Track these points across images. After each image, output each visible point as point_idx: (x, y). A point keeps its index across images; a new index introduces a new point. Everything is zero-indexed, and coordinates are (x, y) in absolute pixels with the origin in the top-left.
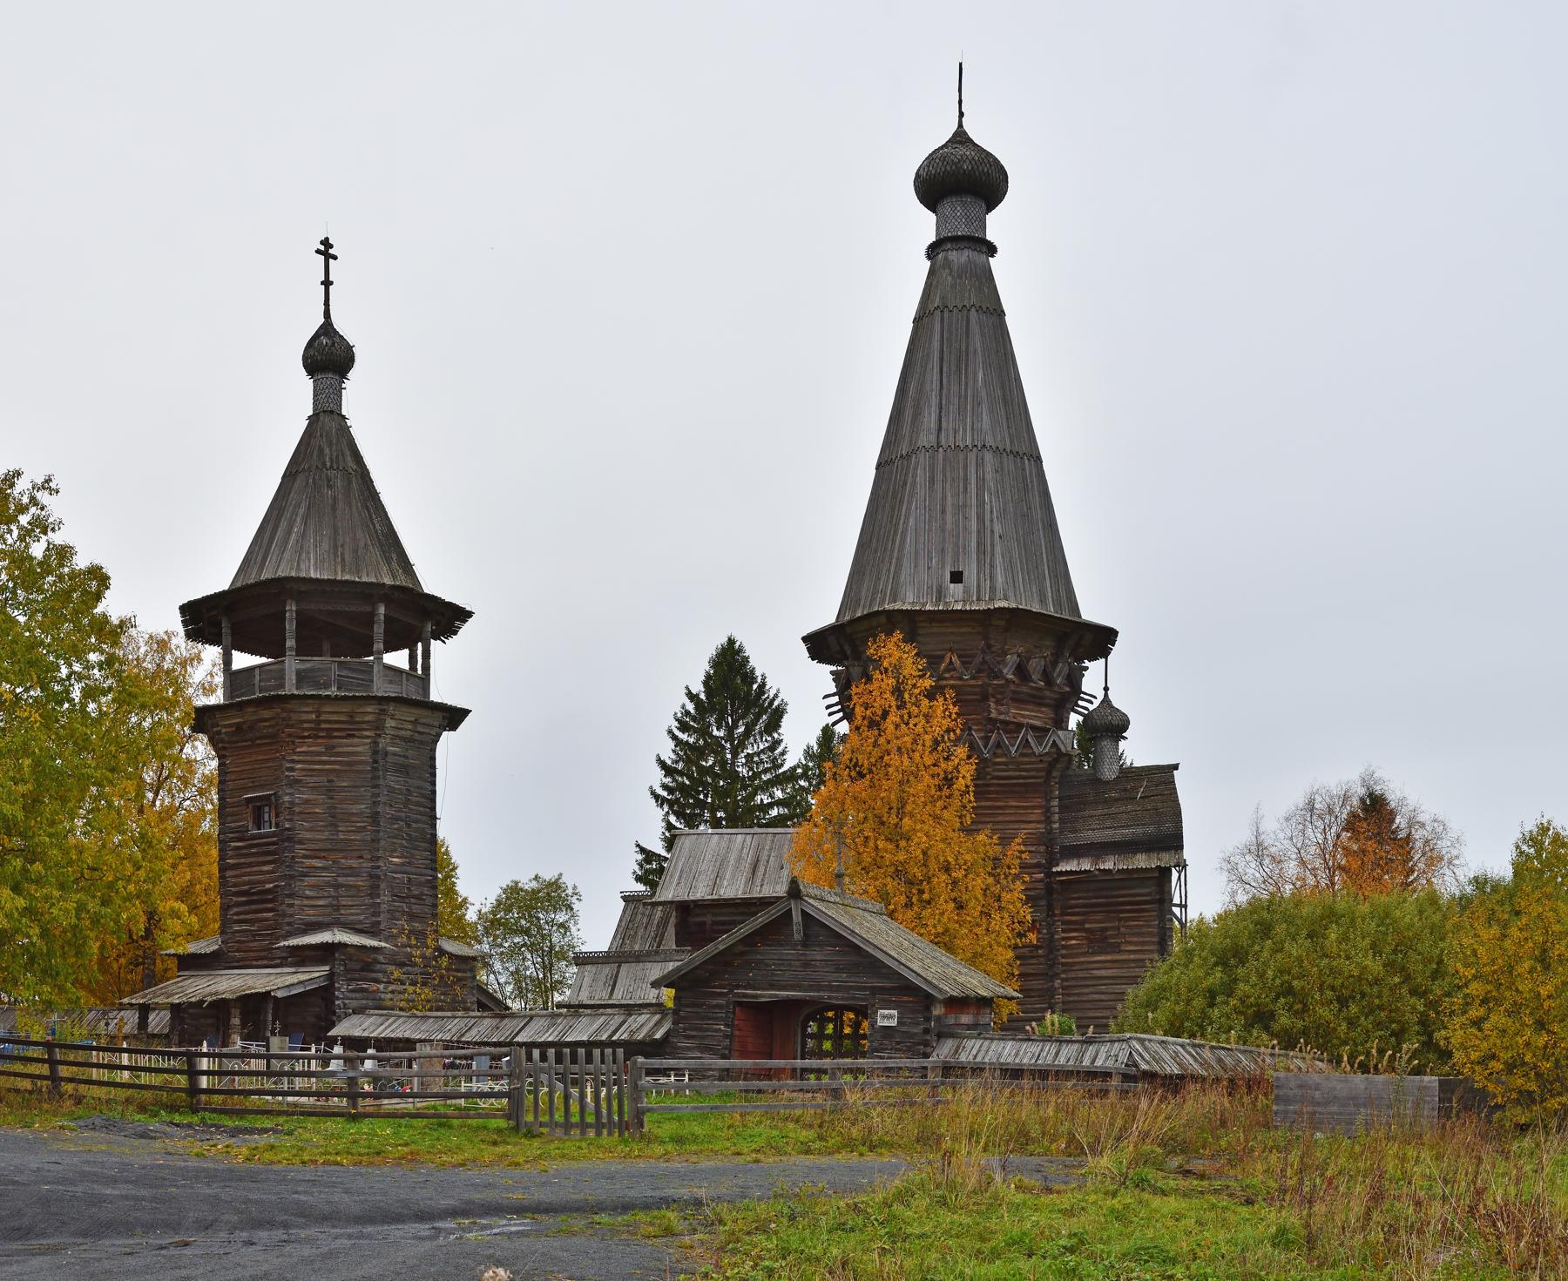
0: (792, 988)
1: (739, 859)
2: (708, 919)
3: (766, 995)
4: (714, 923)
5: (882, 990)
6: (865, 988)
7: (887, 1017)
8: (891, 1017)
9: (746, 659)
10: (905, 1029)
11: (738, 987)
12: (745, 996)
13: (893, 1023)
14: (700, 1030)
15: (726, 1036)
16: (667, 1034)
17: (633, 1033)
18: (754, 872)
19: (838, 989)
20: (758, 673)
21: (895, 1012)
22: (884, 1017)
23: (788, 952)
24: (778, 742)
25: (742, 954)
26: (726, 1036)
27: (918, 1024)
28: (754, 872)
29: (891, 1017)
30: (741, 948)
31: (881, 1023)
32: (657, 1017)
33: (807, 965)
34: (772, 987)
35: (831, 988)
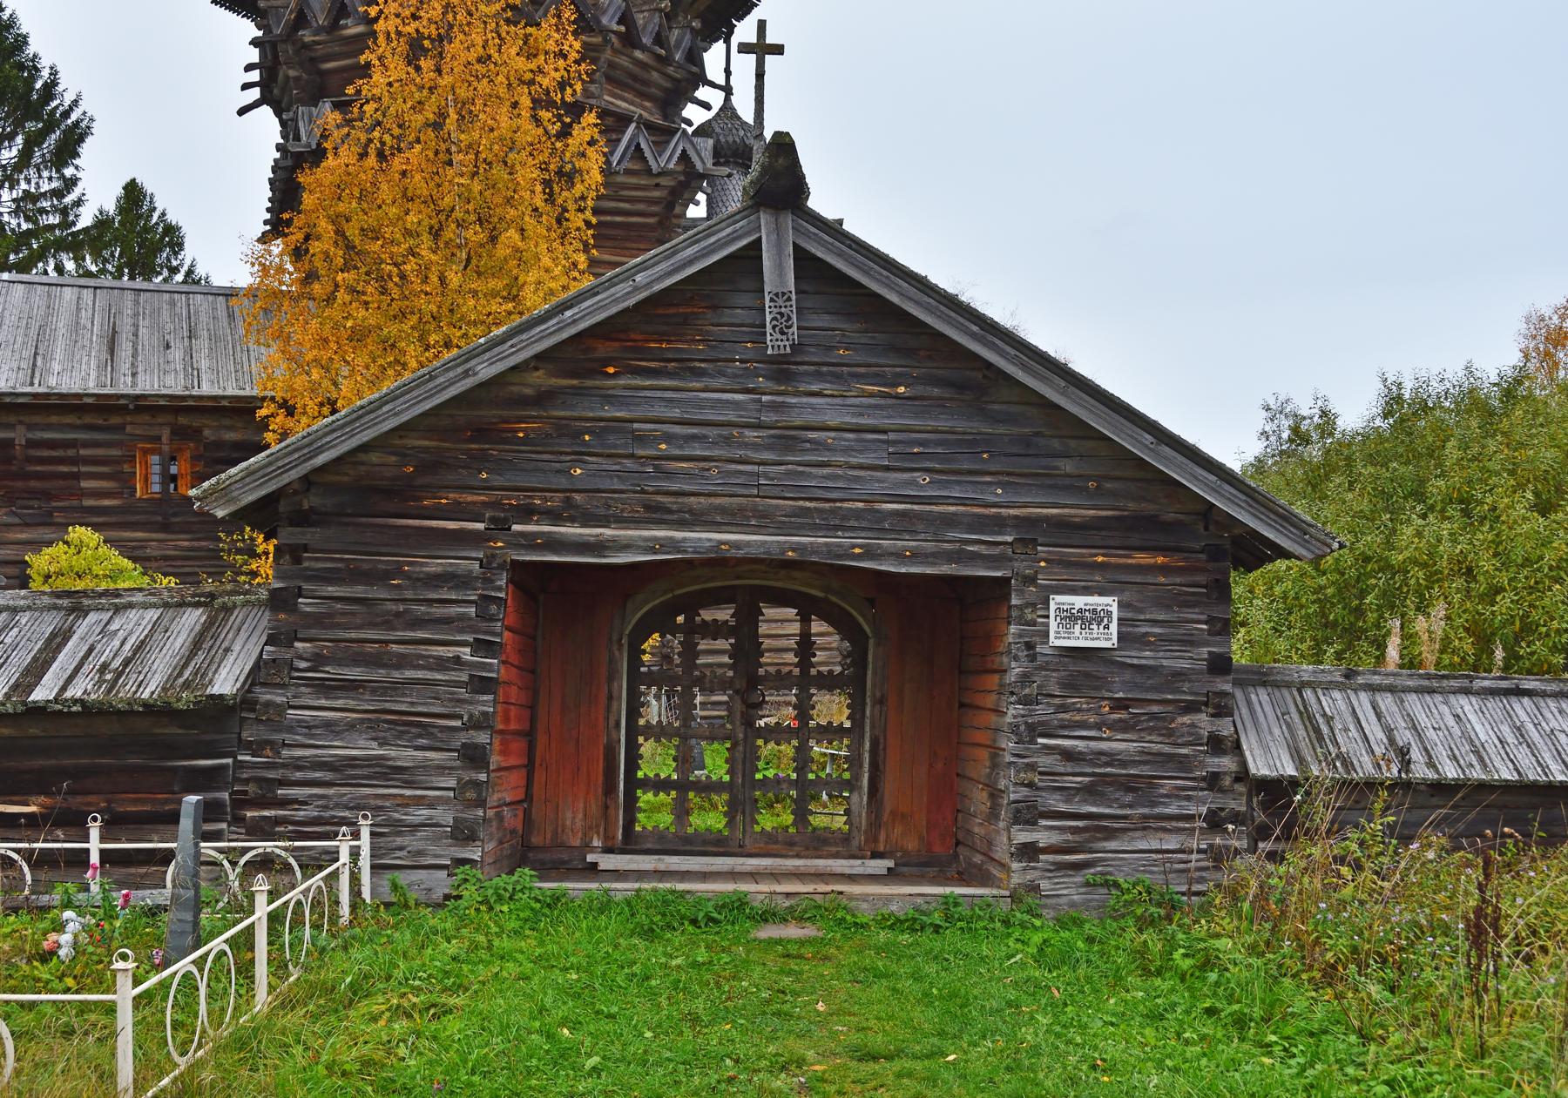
0: (734, 519)
1: (76, 327)
2: (19, 436)
3: (633, 543)
4: (31, 444)
5: (1063, 527)
6: (999, 524)
7: (1083, 619)
8: (1096, 618)
9: (22, 41)
10: (1146, 657)
11: (527, 513)
12: (553, 544)
13: (1105, 638)
14: (374, 661)
15: (482, 685)
16: (258, 674)
17: (111, 675)
18: (112, 351)
19: (905, 523)
20: (45, 64)
21: (1110, 603)
22: (1070, 618)
23: (720, 399)
24: (72, 183)
25: (544, 398)
26: (482, 685)
27: (1190, 642)
28: (112, 351)
29: (1096, 618)
30: (540, 379)
31: (1060, 637)
32: (193, 618)
33: (788, 439)
34: (655, 514)
35: (875, 523)
